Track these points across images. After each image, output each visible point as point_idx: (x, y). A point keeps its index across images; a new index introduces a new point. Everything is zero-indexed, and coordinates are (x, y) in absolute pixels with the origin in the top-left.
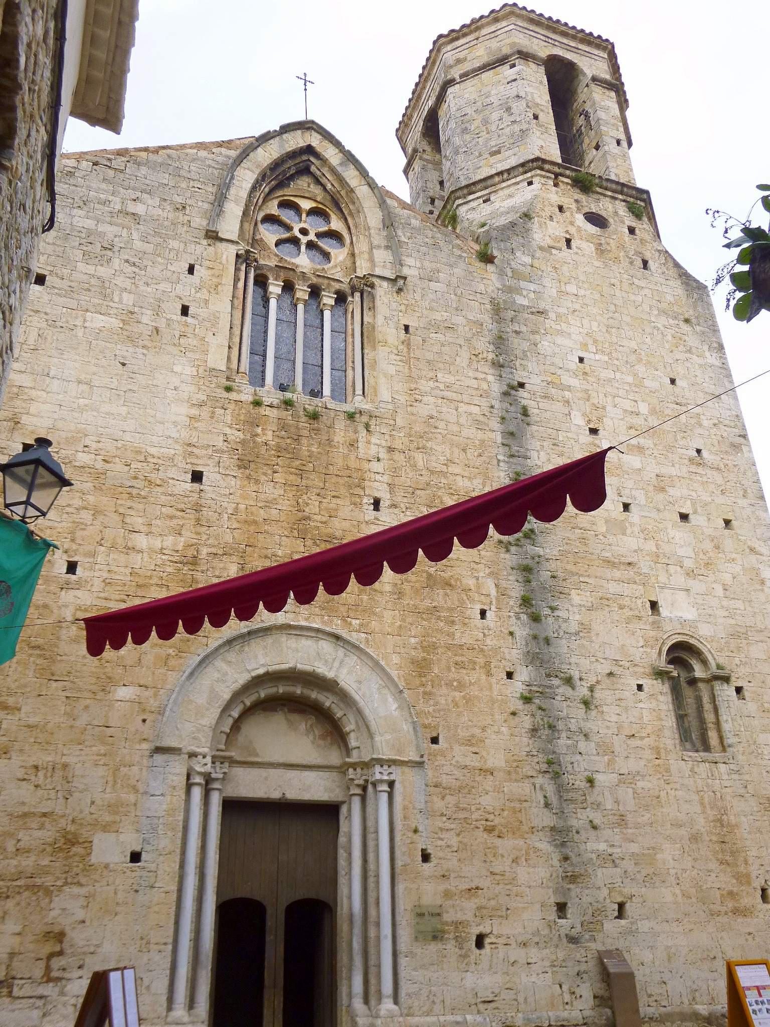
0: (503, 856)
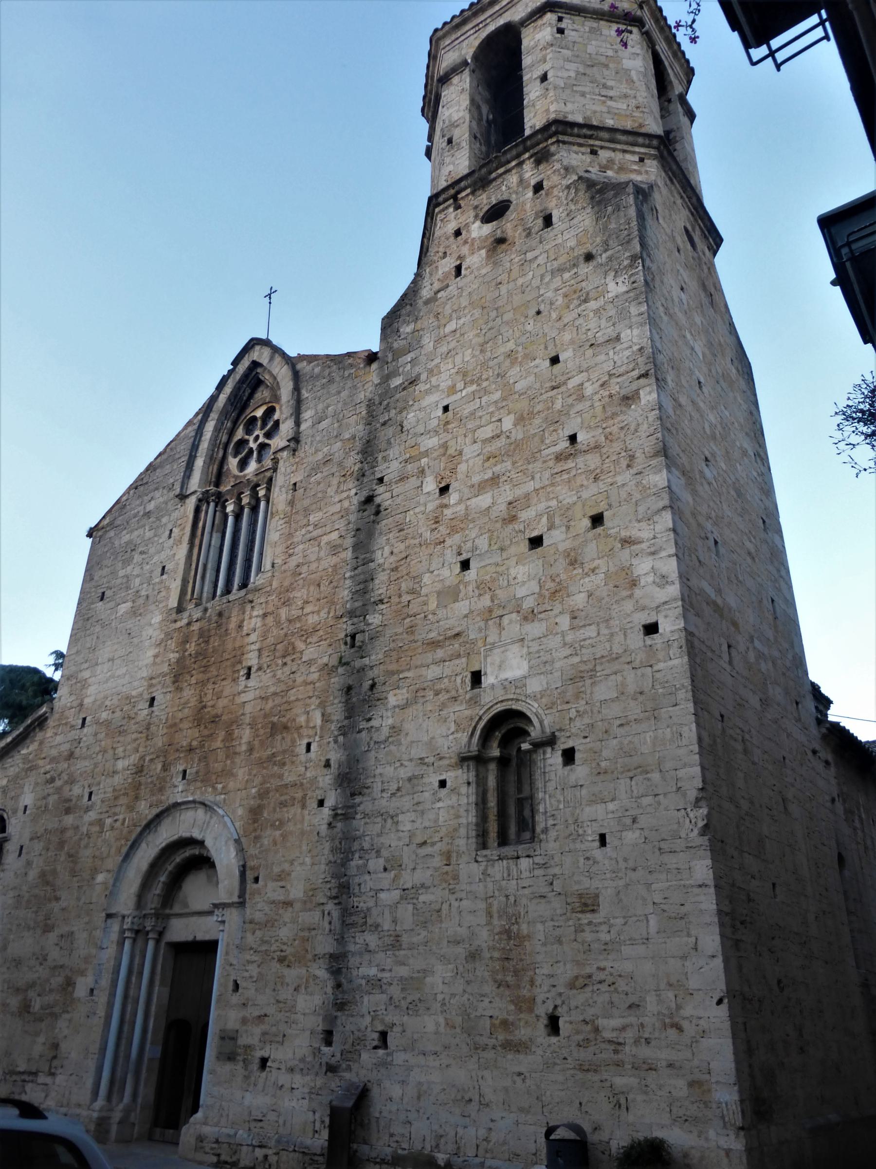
0: (288, 985)
